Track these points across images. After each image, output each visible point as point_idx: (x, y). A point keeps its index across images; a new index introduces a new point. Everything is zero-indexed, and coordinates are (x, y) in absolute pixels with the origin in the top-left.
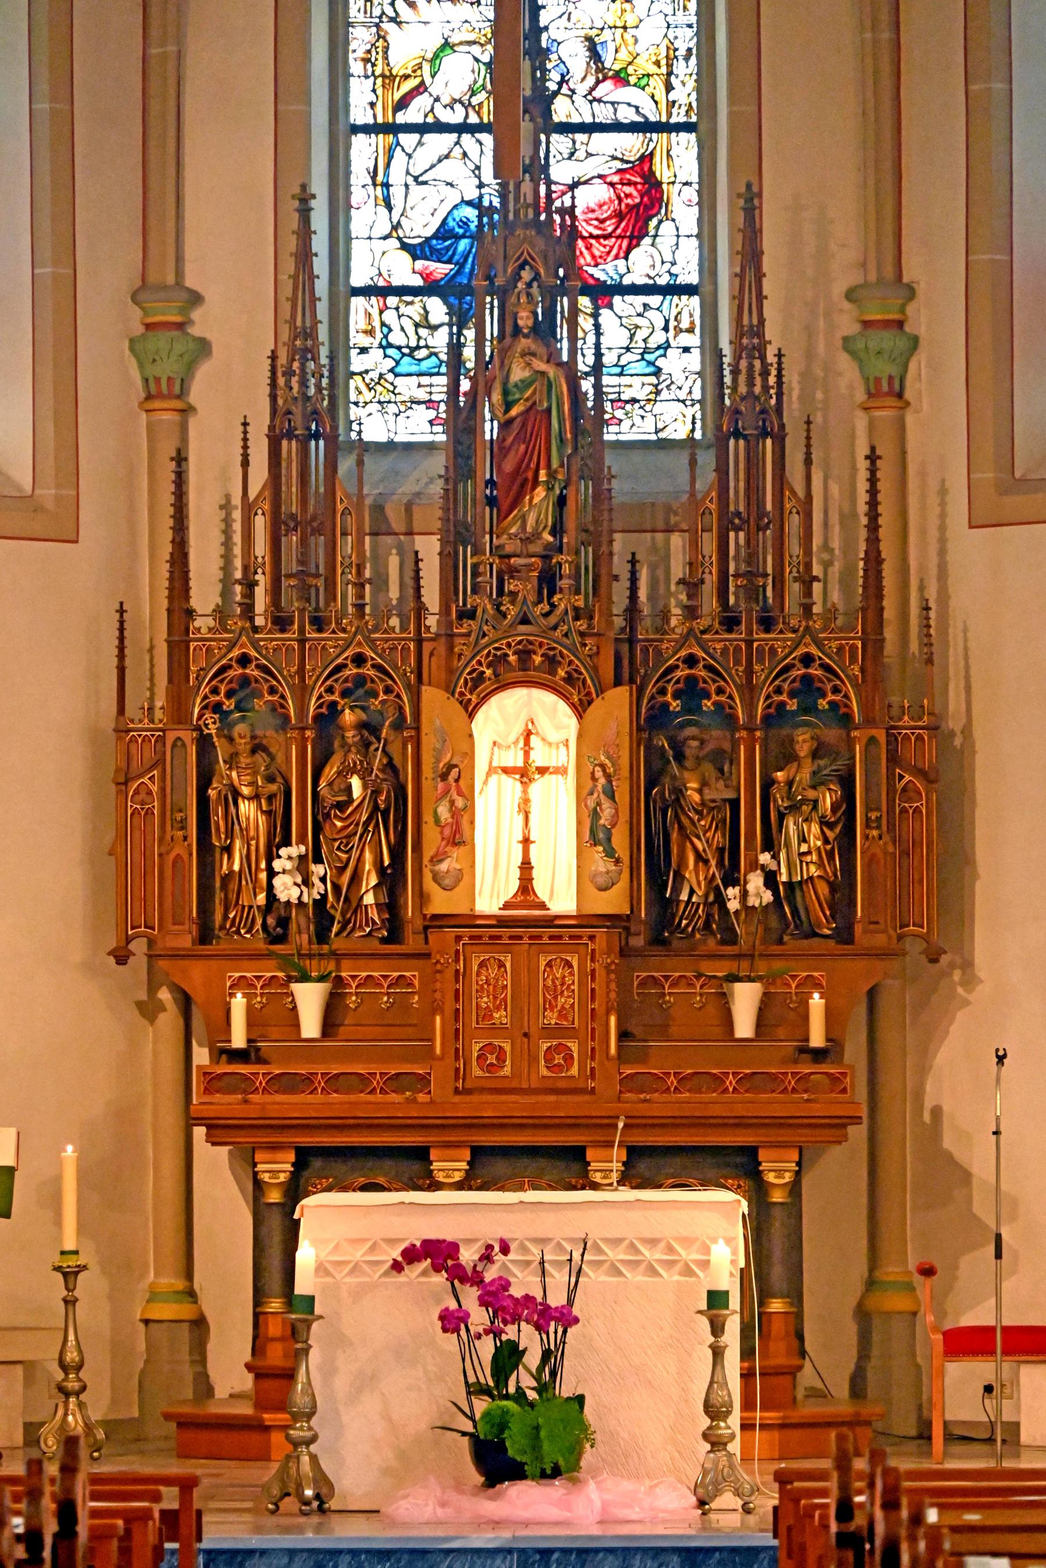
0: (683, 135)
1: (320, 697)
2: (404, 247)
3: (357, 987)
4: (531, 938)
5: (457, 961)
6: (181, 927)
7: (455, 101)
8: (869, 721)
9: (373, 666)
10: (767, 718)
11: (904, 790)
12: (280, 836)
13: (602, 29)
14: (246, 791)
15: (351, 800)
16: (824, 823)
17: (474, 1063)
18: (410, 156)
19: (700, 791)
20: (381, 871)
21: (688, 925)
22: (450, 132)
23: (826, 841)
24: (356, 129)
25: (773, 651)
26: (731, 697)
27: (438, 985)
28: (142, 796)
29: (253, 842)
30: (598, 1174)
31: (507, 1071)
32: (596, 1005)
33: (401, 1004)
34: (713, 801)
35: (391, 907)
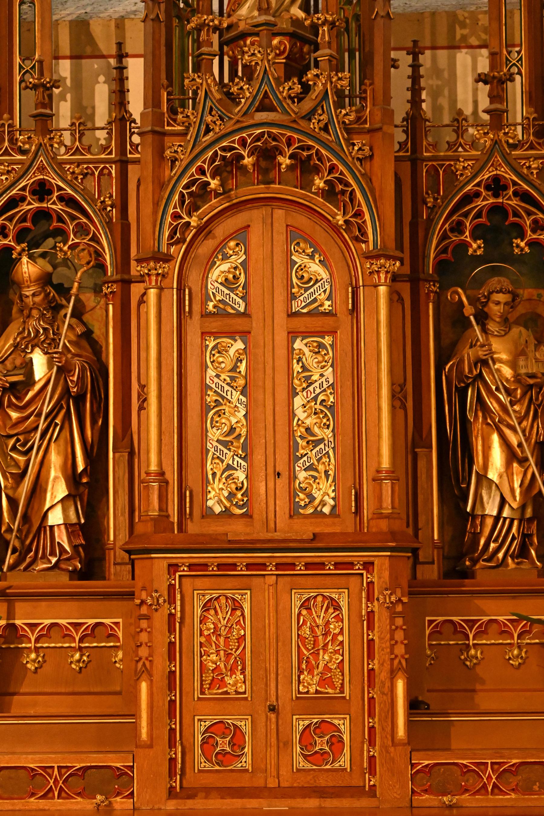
3: (37, 640)
4: (278, 566)
5: (171, 601)
9: (61, 198)
15: (30, 380)
17: (198, 751)
19: (513, 365)
20: (73, 478)
21: (497, 550)
27: (144, 637)
32: (375, 665)
33: (97, 666)
34: (532, 376)
35: (89, 530)
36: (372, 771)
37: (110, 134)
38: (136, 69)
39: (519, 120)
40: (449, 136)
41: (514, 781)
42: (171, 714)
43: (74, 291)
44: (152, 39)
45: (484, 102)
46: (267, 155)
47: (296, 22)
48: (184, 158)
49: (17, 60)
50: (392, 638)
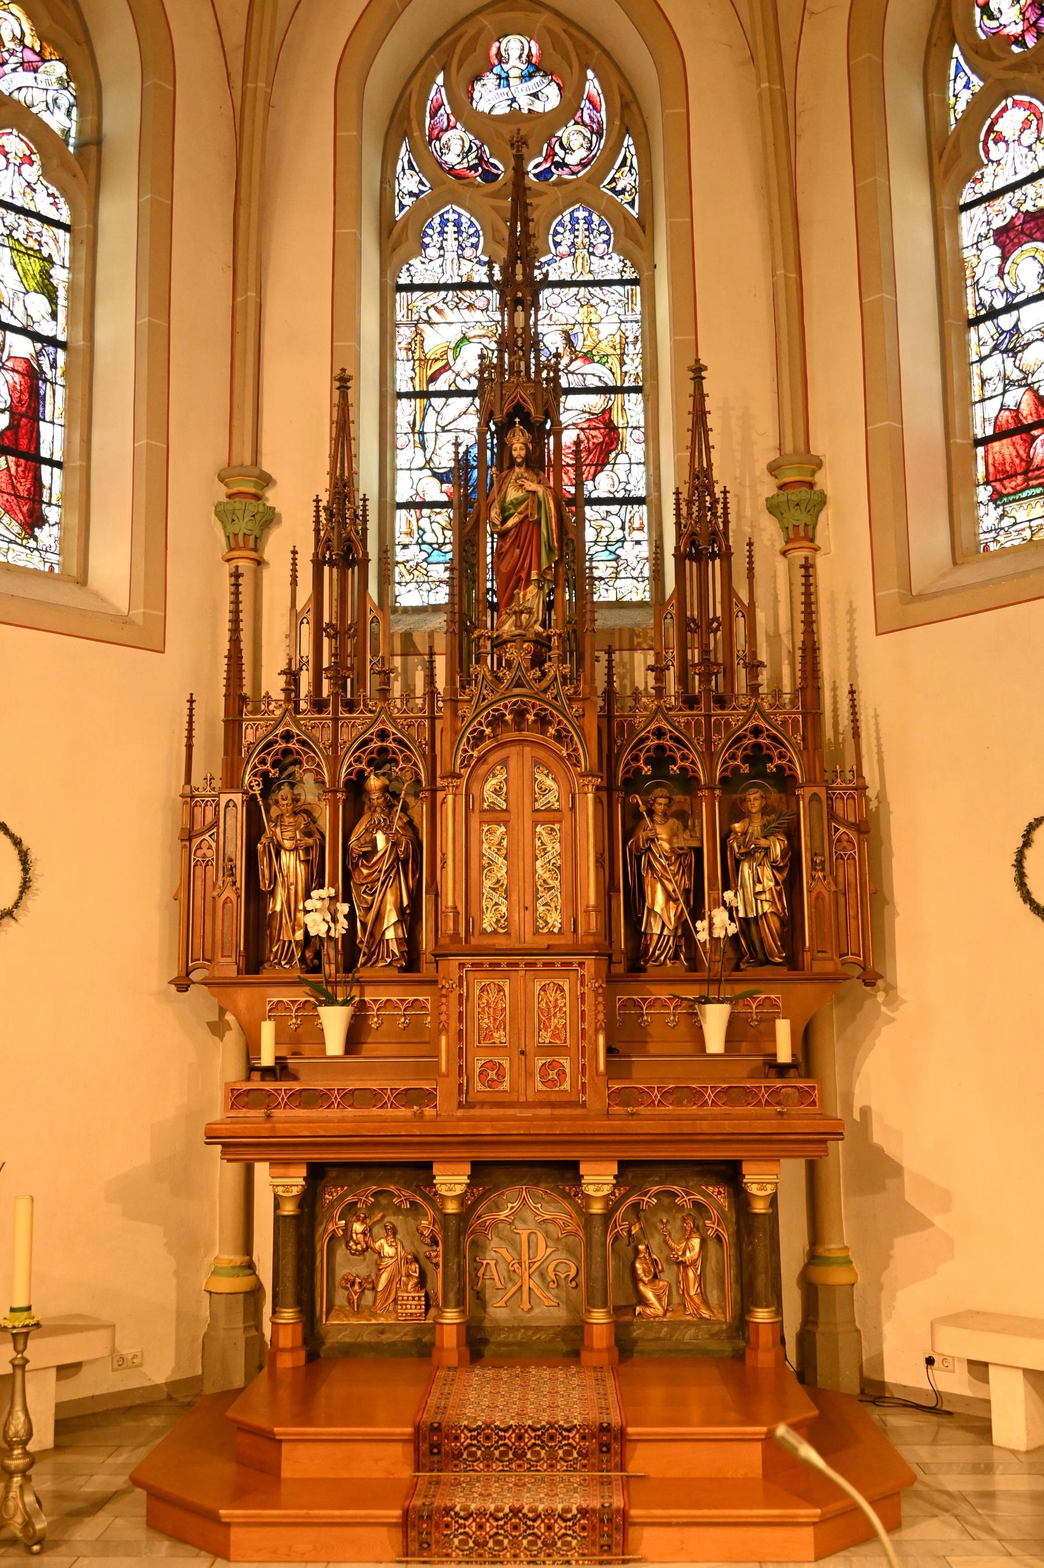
0: (633, 395)
1: (350, 765)
2: (435, 475)
3: (378, 1010)
4: (526, 965)
5: (461, 986)
6: (228, 960)
7: (471, 375)
8: (811, 781)
9: (394, 740)
10: (723, 780)
11: (839, 840)
12: (315, 880)
13: (574, 325)
14: (287, 844)
16: (774, 867)
17: (477, 1079)
18: (439, 413)
19: (670, 842)
20: (401, 910)
22: (468, 396)
23: (777, 883)
24: (400, 395)
25: (728, 724)
26: (693, 762)
27: (444, 1008)
28: (204, 850)
29: (292, 887)
30: (591, 1187)
31: (506, 1086)
32: (586, 1026)
33: (415, 1026)
34: (681, 849)
35: (410, 942)
36: (584, 1092)
37: (424, 701)
38: (441, 664)
39: (673, 693)
40: (630, 703)
41: (671, 1098)
42: (460, 1057)
43: (402, 796)
44: (450, 645)
45: (652, 682)
46: (520, 714)
47: (537, 634)
48: (470, 716)
49: (369, 657)
50: (596, 1009)
